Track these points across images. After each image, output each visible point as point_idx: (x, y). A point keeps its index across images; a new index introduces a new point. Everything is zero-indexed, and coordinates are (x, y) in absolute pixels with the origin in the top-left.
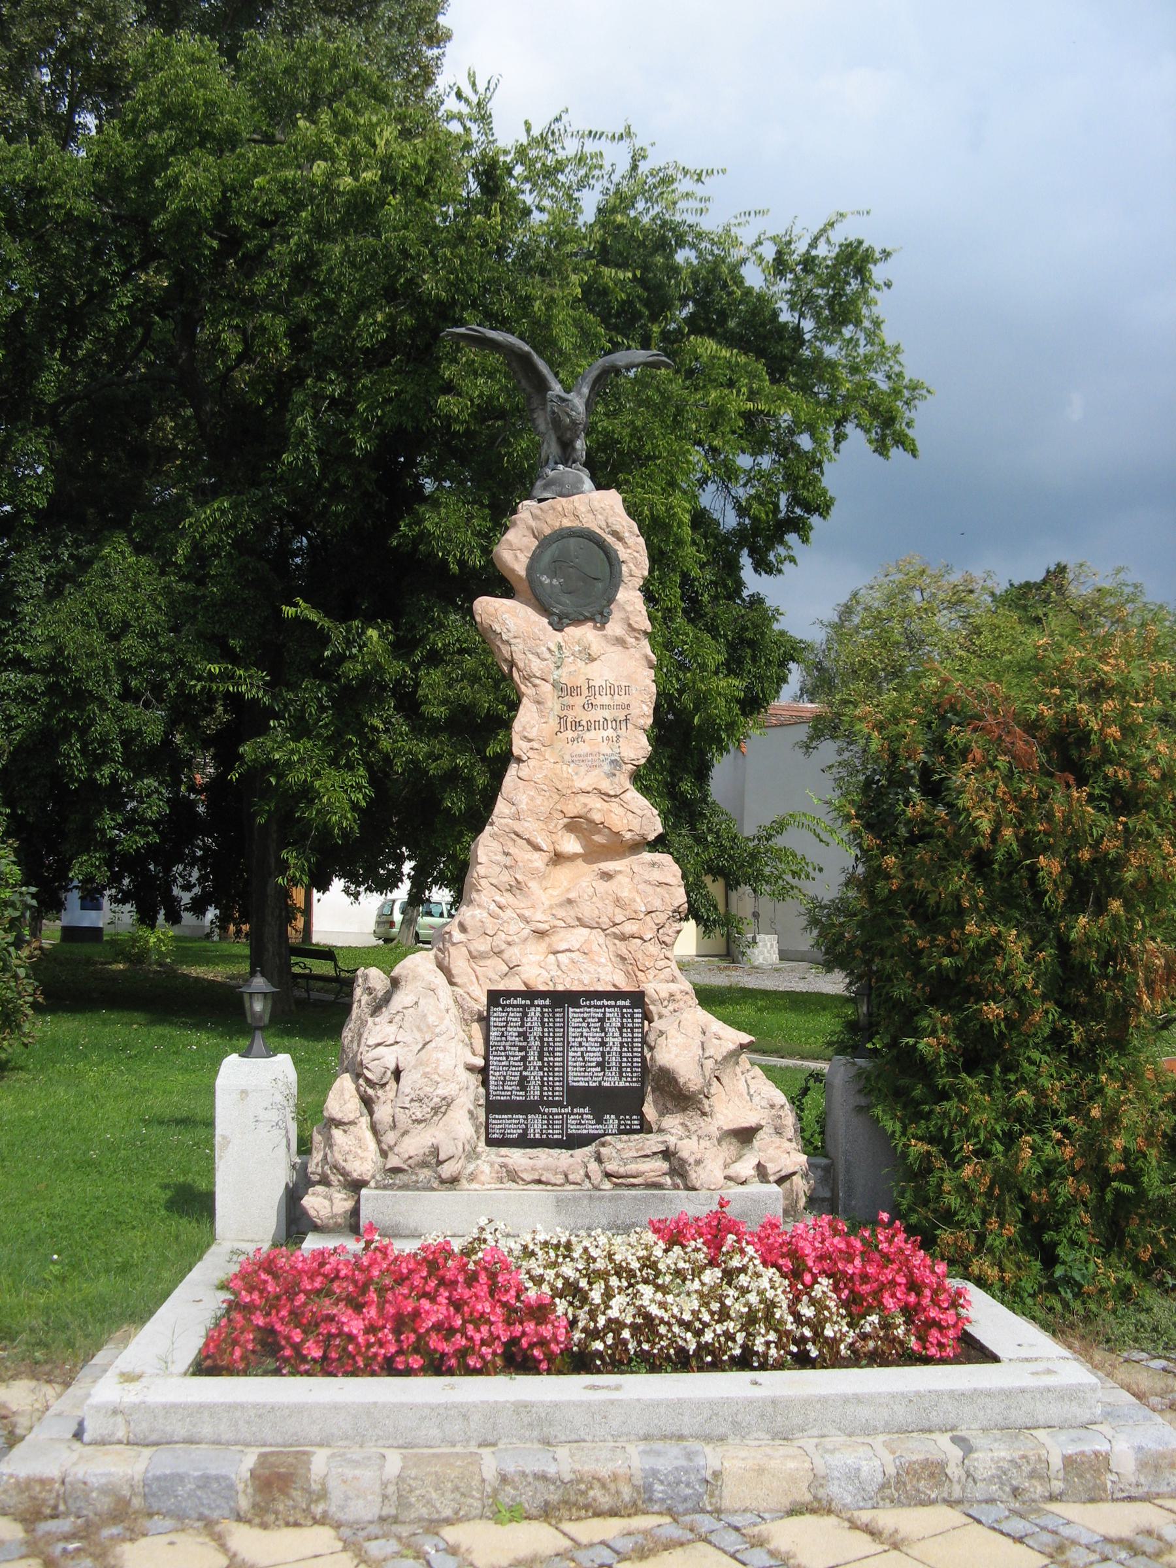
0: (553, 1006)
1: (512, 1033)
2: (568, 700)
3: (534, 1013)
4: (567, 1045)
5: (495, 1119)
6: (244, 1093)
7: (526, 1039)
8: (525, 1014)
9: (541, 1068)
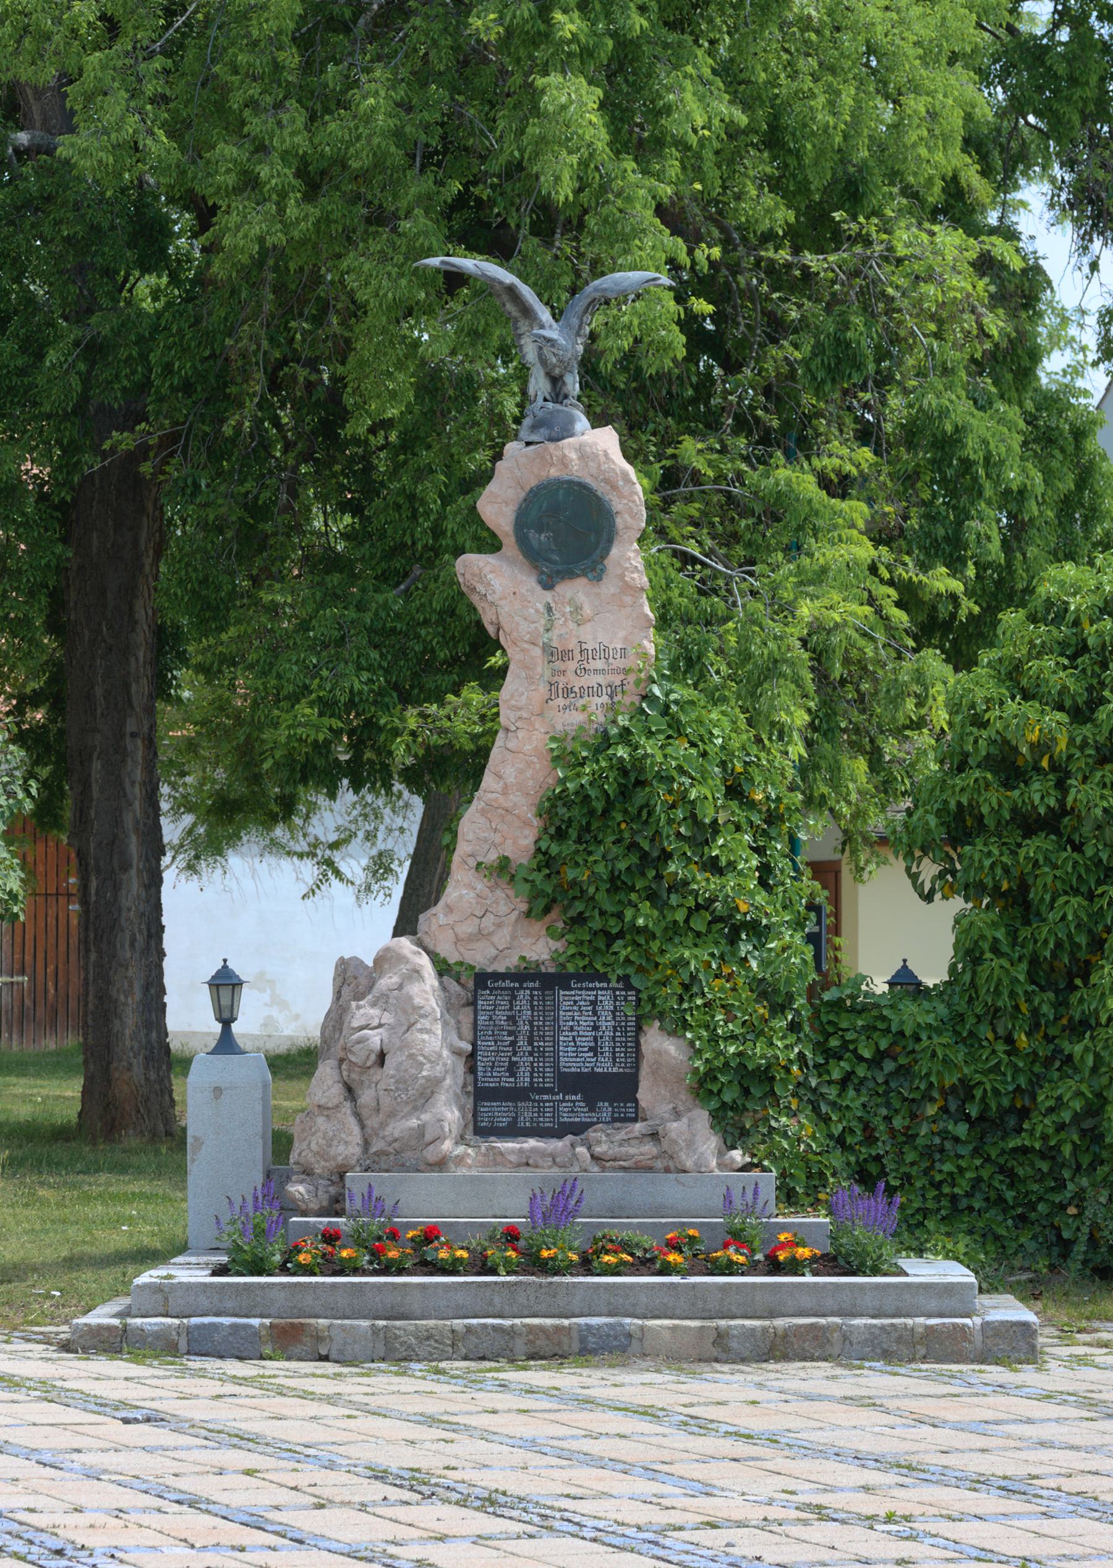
0: (543, 988)
1: (501, 1017)
2: (559, 665)
3: (523, 995)
4: (557, 1029)
5: (486, 1107)
6: (218, 1091)
7: (515, 1023)
8: (514, 997)
9: (531, 1054)
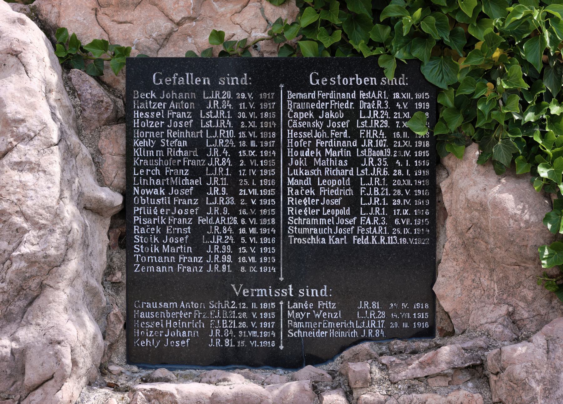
0: (256, 87)
3: (220, 100)
7: (203, 153)
8: (202, 105)
9: (233, 211)
